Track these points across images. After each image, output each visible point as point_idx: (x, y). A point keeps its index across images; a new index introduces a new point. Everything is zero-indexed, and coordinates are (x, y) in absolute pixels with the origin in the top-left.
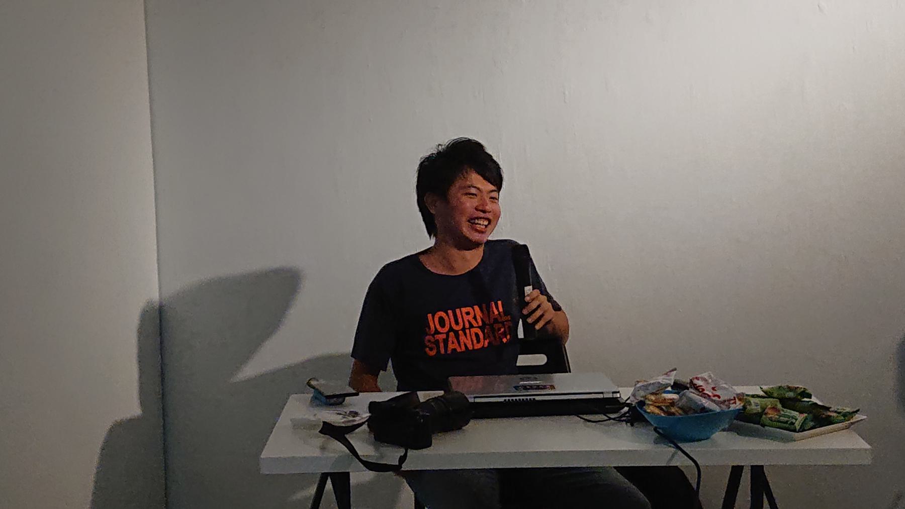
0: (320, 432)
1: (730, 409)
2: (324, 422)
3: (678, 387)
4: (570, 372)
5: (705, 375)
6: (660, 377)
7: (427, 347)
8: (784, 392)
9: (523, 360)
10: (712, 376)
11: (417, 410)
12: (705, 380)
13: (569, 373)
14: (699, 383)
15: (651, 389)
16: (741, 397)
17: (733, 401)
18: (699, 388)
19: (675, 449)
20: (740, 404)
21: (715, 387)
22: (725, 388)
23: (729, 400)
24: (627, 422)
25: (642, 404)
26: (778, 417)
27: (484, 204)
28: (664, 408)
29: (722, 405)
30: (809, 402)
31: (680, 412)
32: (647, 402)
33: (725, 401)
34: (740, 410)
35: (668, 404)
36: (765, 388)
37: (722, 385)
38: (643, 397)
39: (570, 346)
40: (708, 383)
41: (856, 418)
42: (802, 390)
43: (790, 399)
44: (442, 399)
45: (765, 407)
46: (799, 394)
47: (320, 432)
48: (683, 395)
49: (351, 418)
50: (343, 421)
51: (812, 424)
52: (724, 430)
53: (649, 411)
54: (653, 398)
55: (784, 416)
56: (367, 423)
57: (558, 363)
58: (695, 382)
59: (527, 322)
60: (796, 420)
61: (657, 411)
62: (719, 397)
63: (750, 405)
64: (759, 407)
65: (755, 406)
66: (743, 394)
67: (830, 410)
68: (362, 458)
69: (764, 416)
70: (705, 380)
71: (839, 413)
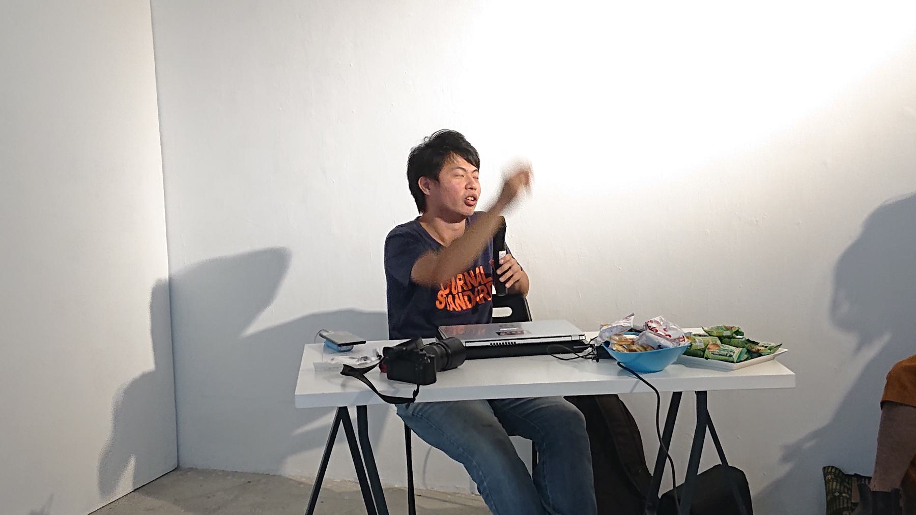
0: (341, 373)
1: (680, 346)
2: (344, 365)
3: (632, 330)
4: (531, 321)
5: (657, 319)
6: (621, 321)
7: (438, 300)
8: (722, 331)
9: (498, 312)
10: (663, 319)
11: (424, 352)
12: (658, 323)
13: (530, 322)
14: (653, 325)
15: (615, 331)
16: (689, 336)
17: (681, 340)
18: (653, 329)
19: (637, 379)
20: (688, 341)
21: (666, 328)
22: (674, 329)
23: (679, 338)
24: (593, 359)
25: (607, 343)
26: (719, 351)
27: (470, 183)
28: (624, 346)
29: (674, 343)
30: (742, 338)
31: (641, 348)
32: (612, 341)
33: (675, 339)
34: (688, 346)
35: (629, 343)
36: (706, 329)
37: (671, 327)
38: (608, 338)
39: (531, 299)
40: (661, 325)
41: (782, 350)
42: (737, 329)
43: (729, 337)
44: (445, 346)
45: (708, 343)
46: (735, 332)
47: (341, 373)
48: (643, 335)
49: (363, 362)
50: (358, 363)
51: (746, 356)
52: (674, 363)
53: (614, 349)
54: (617, 338)
55: (724, 350)
56: (378, 365)
57: (521, 314)
58: (650, 324)
59: (500, 282)
60: (734, 353)
61: (620, 348)
62: (670, 336)
63: (695, 342)
64: (702, 344)
65: (699, 344)
66: (690, 333)
67: (759, 345)
68: (379, 392)
69: (707, 351)
70: (658, 323)
71: (766, 347)
